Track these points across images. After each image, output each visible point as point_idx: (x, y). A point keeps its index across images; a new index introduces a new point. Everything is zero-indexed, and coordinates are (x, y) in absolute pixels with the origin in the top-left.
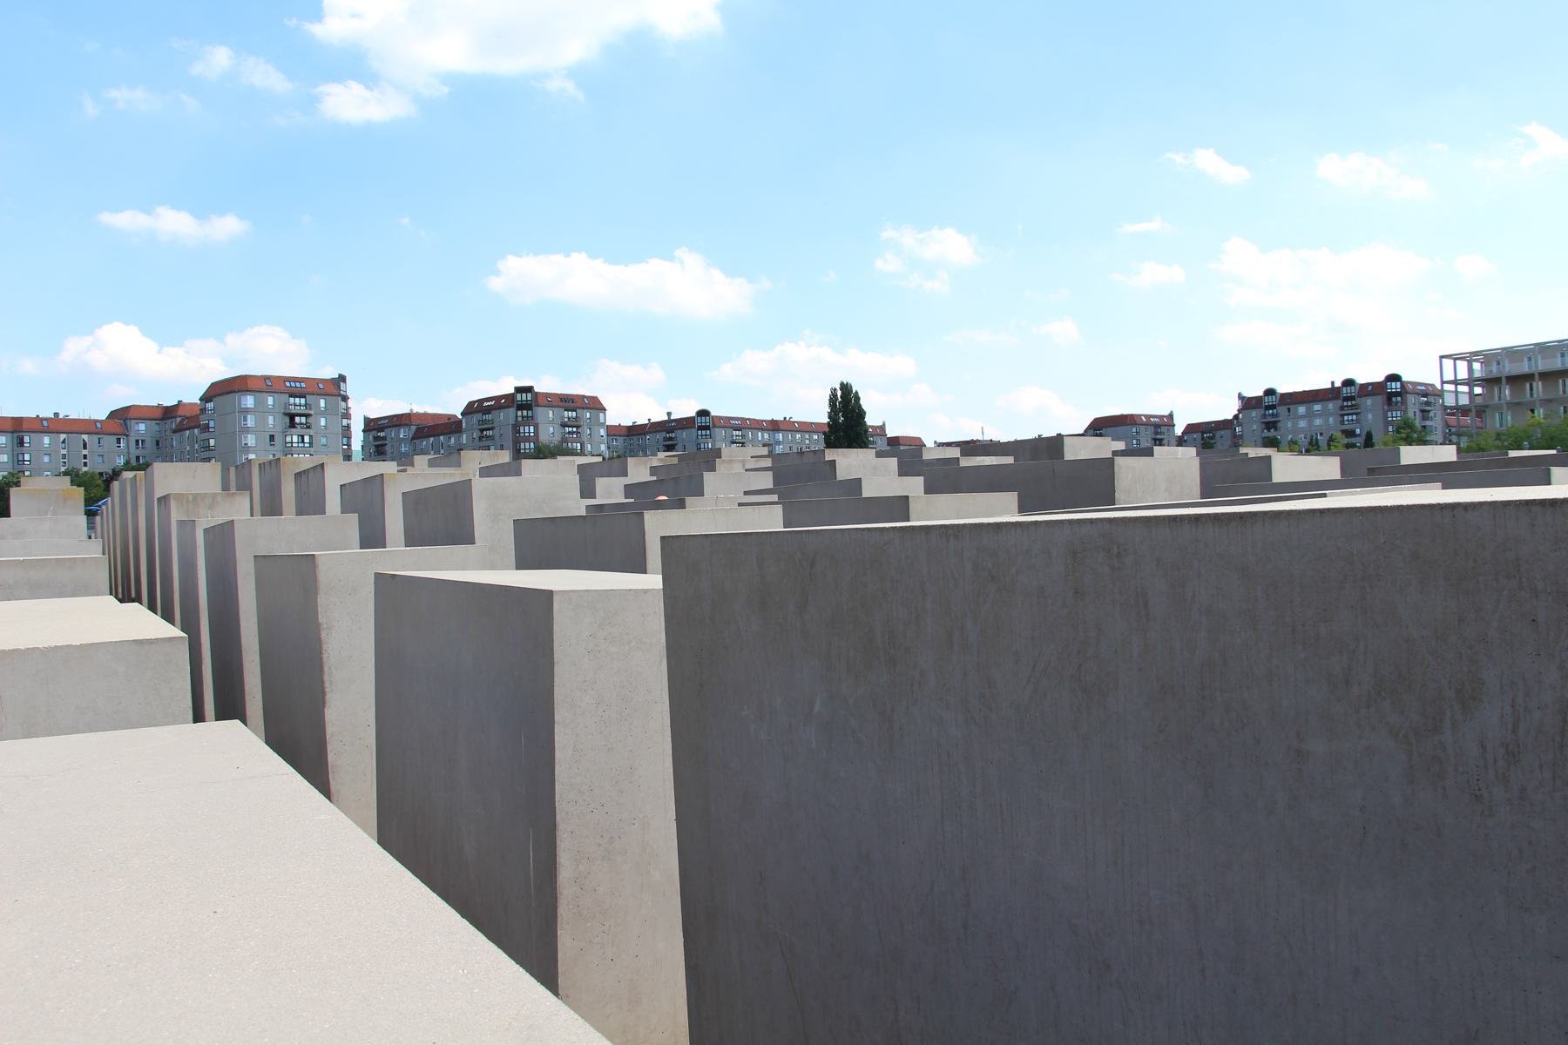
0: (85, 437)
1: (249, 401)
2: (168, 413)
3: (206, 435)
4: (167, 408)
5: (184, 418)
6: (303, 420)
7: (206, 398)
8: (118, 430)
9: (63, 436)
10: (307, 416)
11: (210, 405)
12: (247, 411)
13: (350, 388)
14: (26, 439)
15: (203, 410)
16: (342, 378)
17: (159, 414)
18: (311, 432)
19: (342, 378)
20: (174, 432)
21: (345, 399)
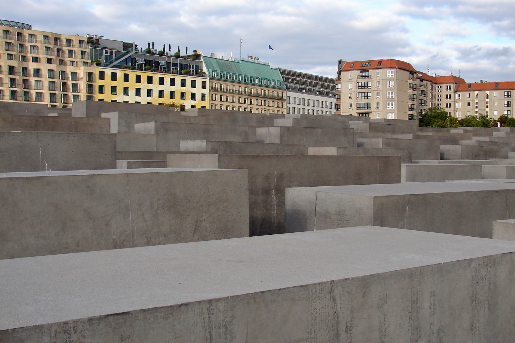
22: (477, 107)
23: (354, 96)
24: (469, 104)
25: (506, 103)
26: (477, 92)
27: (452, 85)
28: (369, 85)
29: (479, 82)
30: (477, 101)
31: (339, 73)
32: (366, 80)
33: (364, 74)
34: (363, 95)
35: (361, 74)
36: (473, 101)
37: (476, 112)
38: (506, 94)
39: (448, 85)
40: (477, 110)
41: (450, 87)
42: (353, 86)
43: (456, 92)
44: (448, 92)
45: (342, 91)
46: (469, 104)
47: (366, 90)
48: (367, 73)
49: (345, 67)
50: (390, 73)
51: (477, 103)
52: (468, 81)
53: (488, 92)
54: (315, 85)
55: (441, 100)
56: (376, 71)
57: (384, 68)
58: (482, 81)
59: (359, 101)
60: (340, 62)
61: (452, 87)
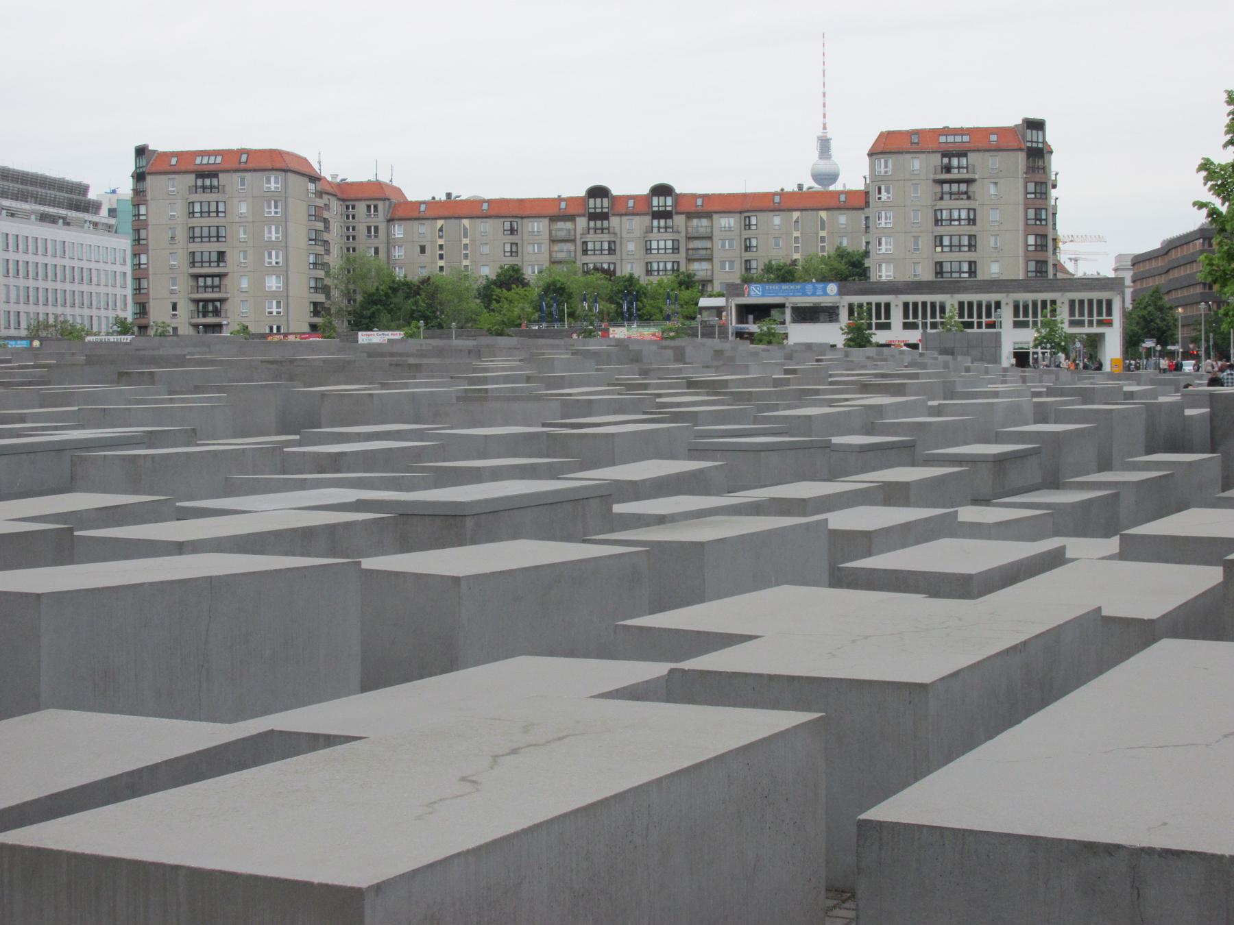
0: (823, 214)
6: (963, 187)
9: (796, 215)
10: (969, 182)
14: (754, 221)
22: (441, 257)
23: (182, 235)
24: (423, 249)
25: (508, 248)
26: (440, 223)
27: (380, 205)
28: (221, 208)
29: (444, 198)
30: (441, 242)
31: (139, 177)
32: (212, 197)
33: (208, 182)
34: (205, 233)
35: (200, 182)
36: (434, 242)
37: (441, 268)
38: (507, 226)
39: (372, 203)
40: (441, 263)
41: (376, 207)
42: (179, 211)
43: (390, 220)
44: (372, 221)
45: (151, 221)
46: (423, 249)
47: (213, 221)
48: (215, 182)
49: (148, 164)
50: (273, 183)
51: (441, 247)
52: (412, 195)
53: (466, 222)
54: (21, 196)
55: (354, 238)
56: (236, 176)
57: (255, 170)
58: (449, 195)
59: (195, 247)
60: (141, 151)
61: (380, 208)
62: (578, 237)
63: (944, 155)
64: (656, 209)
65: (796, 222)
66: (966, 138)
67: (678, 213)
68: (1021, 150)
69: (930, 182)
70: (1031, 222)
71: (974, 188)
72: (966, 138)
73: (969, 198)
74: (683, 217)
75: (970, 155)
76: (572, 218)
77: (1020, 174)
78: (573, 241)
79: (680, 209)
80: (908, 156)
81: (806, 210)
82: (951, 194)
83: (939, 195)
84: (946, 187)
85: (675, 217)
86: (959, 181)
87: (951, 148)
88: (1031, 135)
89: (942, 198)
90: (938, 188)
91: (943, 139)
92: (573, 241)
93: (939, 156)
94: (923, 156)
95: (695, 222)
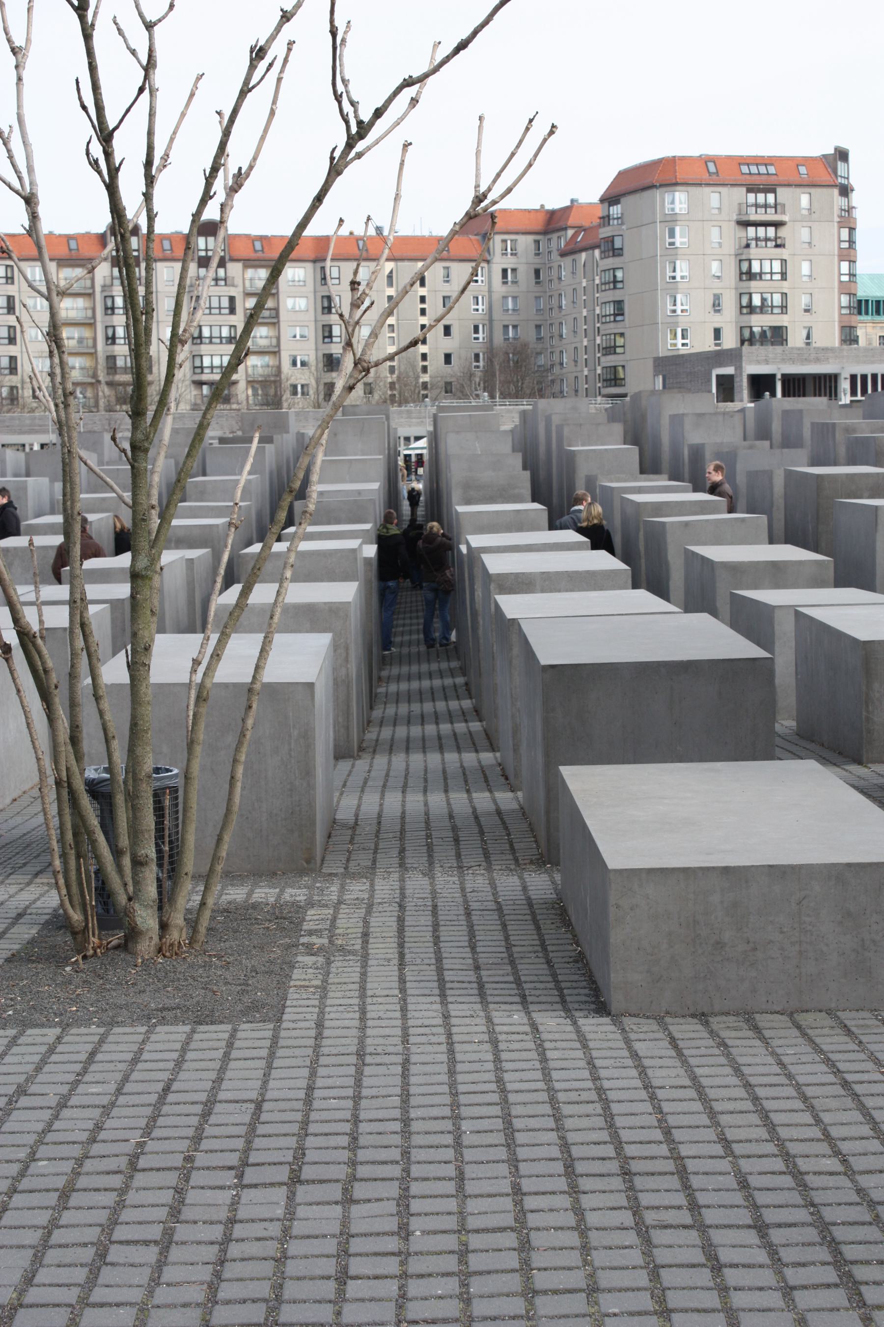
1: (679, 201)
2: (552, 222)
3: (610, 262)
4: (552, 214)
5: (579, 228)
6: (771, 231)
7: (611, 198)
8: (474, 254)
10: (777, 225)
11: (616, 210)
12: (671, 221)
13: (856, 172)
15: (606, 219)
16: (842, 155)
17: (539, 227)
18: (784, 253)
19: (842, 155)
20: (563, 254)
21: (845, 191)
62: (98, 289)
63: (749, 191)
64: (203, 254)
65: (390, 277)
66: (772, 170)
67: (232, 260)
68: (835, 186)
69: (733, 224)
70: (845, 278)
71: (783, 232)
72: (772, 170)
73: (777, 246)
74: (239, 266)
75: (779, 190)
76: (88, 264)
77: (837, 219)
78: (90, 295)
79: (236, 254)
80: (707, 190)
81: (402, 260)
82: (757, 239)
83: (744, 242)
84: (751, 230)
85: (230, 266)
86: (766, 224)
87: (756, 180)
88: (840, 165)
89: (748, 246)
90: (741, 233)
91: (745, 169)
92: (90, 295)
93: (744, 189)
94: (724, 190)
95: (250, 273)
